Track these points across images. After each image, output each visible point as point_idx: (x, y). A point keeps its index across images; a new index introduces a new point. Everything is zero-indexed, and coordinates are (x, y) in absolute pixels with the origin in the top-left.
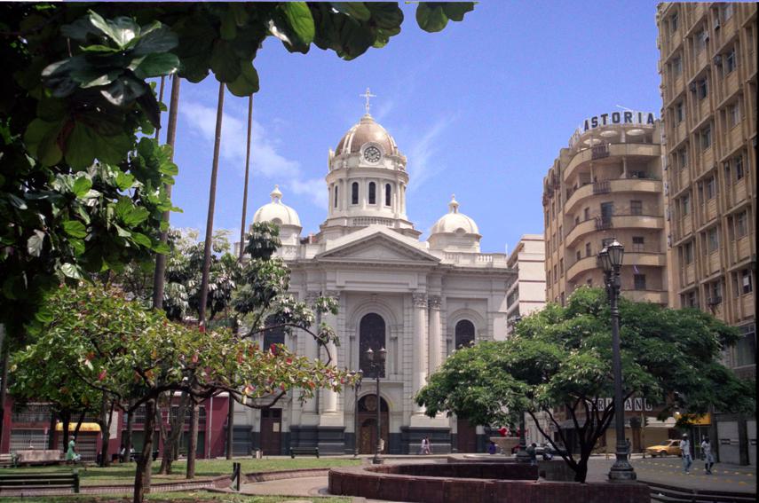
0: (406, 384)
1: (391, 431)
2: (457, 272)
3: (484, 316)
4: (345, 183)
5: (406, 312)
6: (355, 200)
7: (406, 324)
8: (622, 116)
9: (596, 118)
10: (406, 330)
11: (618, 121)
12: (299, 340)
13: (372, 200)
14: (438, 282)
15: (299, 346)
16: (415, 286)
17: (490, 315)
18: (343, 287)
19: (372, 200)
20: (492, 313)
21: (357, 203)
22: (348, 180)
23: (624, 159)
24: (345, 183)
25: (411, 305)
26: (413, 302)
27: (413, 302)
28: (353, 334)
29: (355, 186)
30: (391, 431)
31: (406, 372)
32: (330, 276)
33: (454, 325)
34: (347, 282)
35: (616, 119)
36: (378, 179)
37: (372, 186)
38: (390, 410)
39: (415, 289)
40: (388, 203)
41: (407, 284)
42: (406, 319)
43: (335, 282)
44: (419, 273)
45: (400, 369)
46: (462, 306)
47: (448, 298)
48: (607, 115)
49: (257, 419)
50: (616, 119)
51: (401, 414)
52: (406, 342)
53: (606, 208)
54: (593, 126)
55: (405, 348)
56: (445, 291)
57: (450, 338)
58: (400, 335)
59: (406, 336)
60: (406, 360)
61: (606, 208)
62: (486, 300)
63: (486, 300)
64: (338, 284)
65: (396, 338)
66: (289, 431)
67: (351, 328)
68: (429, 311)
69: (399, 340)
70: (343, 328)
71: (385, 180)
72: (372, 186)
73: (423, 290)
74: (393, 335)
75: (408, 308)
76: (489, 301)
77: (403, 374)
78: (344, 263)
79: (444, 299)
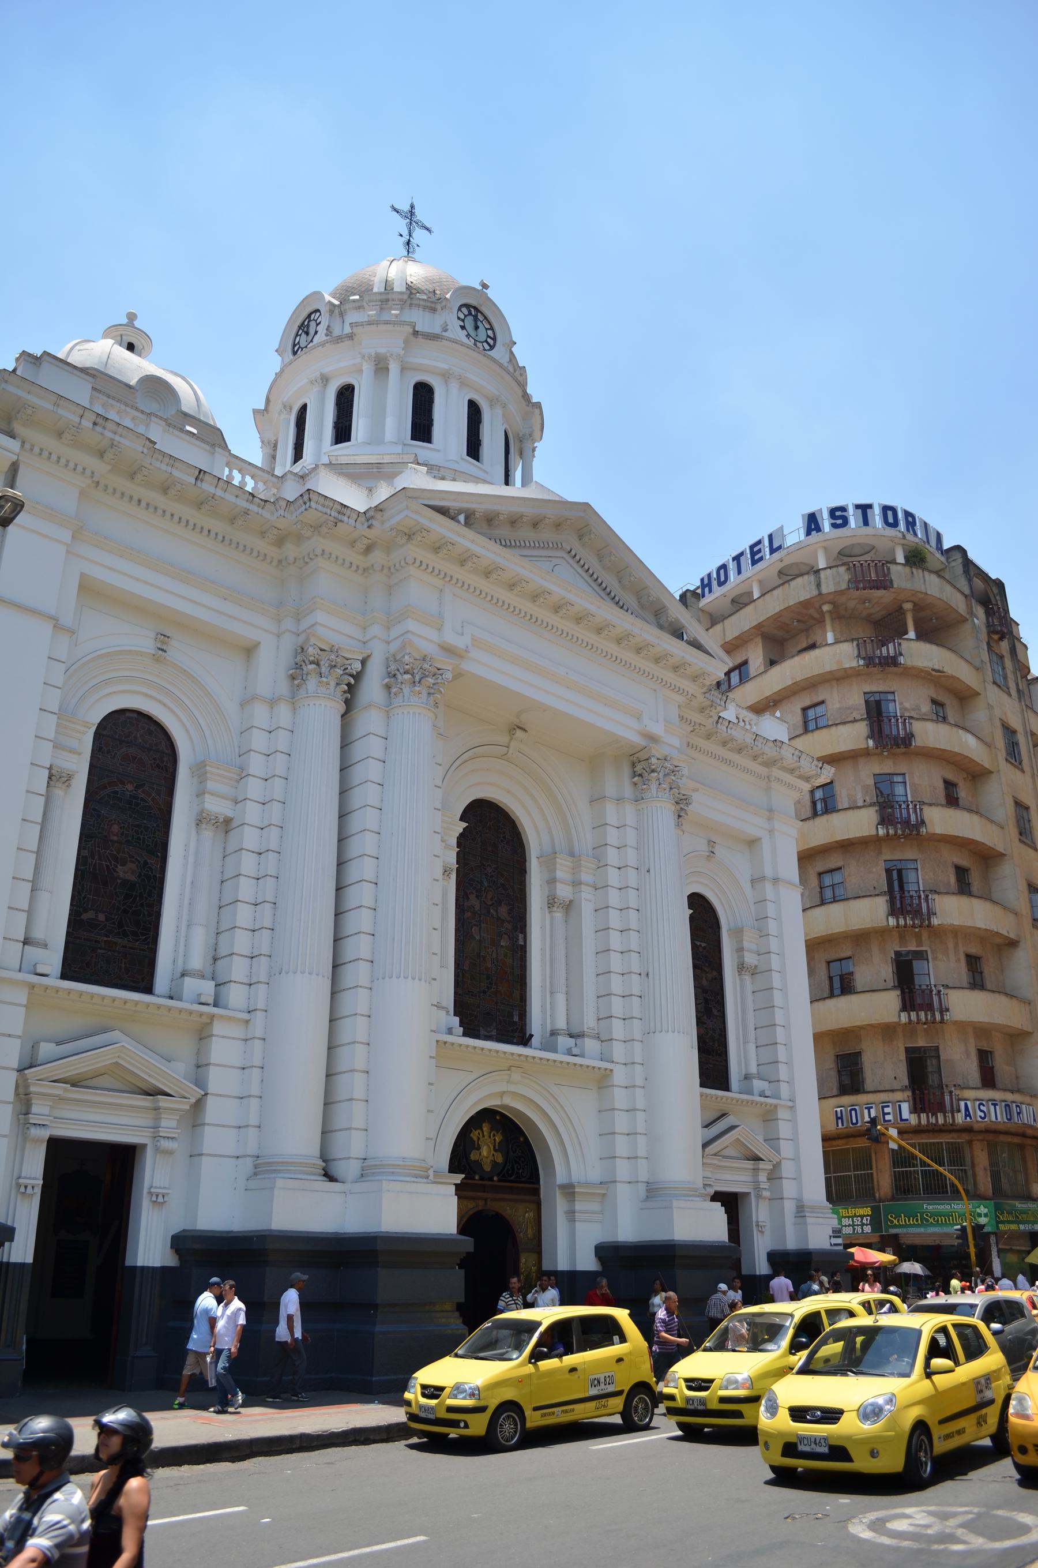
0: (619, 1076)
5: (611, 813)
8: (900, 515)
9: (843, 509)
11: (895, 524)
12: (250, 838)
15: (248, 864)
23: (908, 606)
31: (618, 1029)
35: (891, 520)
48: (870, 506)
49: (20, 1188)
50: (891, 520)
53: (878, 703)
54: (834, 526)
61: (878, 703)
64: (451, 638)
66: (170, 1260)
69: (587, 910)
72: (474, 413)
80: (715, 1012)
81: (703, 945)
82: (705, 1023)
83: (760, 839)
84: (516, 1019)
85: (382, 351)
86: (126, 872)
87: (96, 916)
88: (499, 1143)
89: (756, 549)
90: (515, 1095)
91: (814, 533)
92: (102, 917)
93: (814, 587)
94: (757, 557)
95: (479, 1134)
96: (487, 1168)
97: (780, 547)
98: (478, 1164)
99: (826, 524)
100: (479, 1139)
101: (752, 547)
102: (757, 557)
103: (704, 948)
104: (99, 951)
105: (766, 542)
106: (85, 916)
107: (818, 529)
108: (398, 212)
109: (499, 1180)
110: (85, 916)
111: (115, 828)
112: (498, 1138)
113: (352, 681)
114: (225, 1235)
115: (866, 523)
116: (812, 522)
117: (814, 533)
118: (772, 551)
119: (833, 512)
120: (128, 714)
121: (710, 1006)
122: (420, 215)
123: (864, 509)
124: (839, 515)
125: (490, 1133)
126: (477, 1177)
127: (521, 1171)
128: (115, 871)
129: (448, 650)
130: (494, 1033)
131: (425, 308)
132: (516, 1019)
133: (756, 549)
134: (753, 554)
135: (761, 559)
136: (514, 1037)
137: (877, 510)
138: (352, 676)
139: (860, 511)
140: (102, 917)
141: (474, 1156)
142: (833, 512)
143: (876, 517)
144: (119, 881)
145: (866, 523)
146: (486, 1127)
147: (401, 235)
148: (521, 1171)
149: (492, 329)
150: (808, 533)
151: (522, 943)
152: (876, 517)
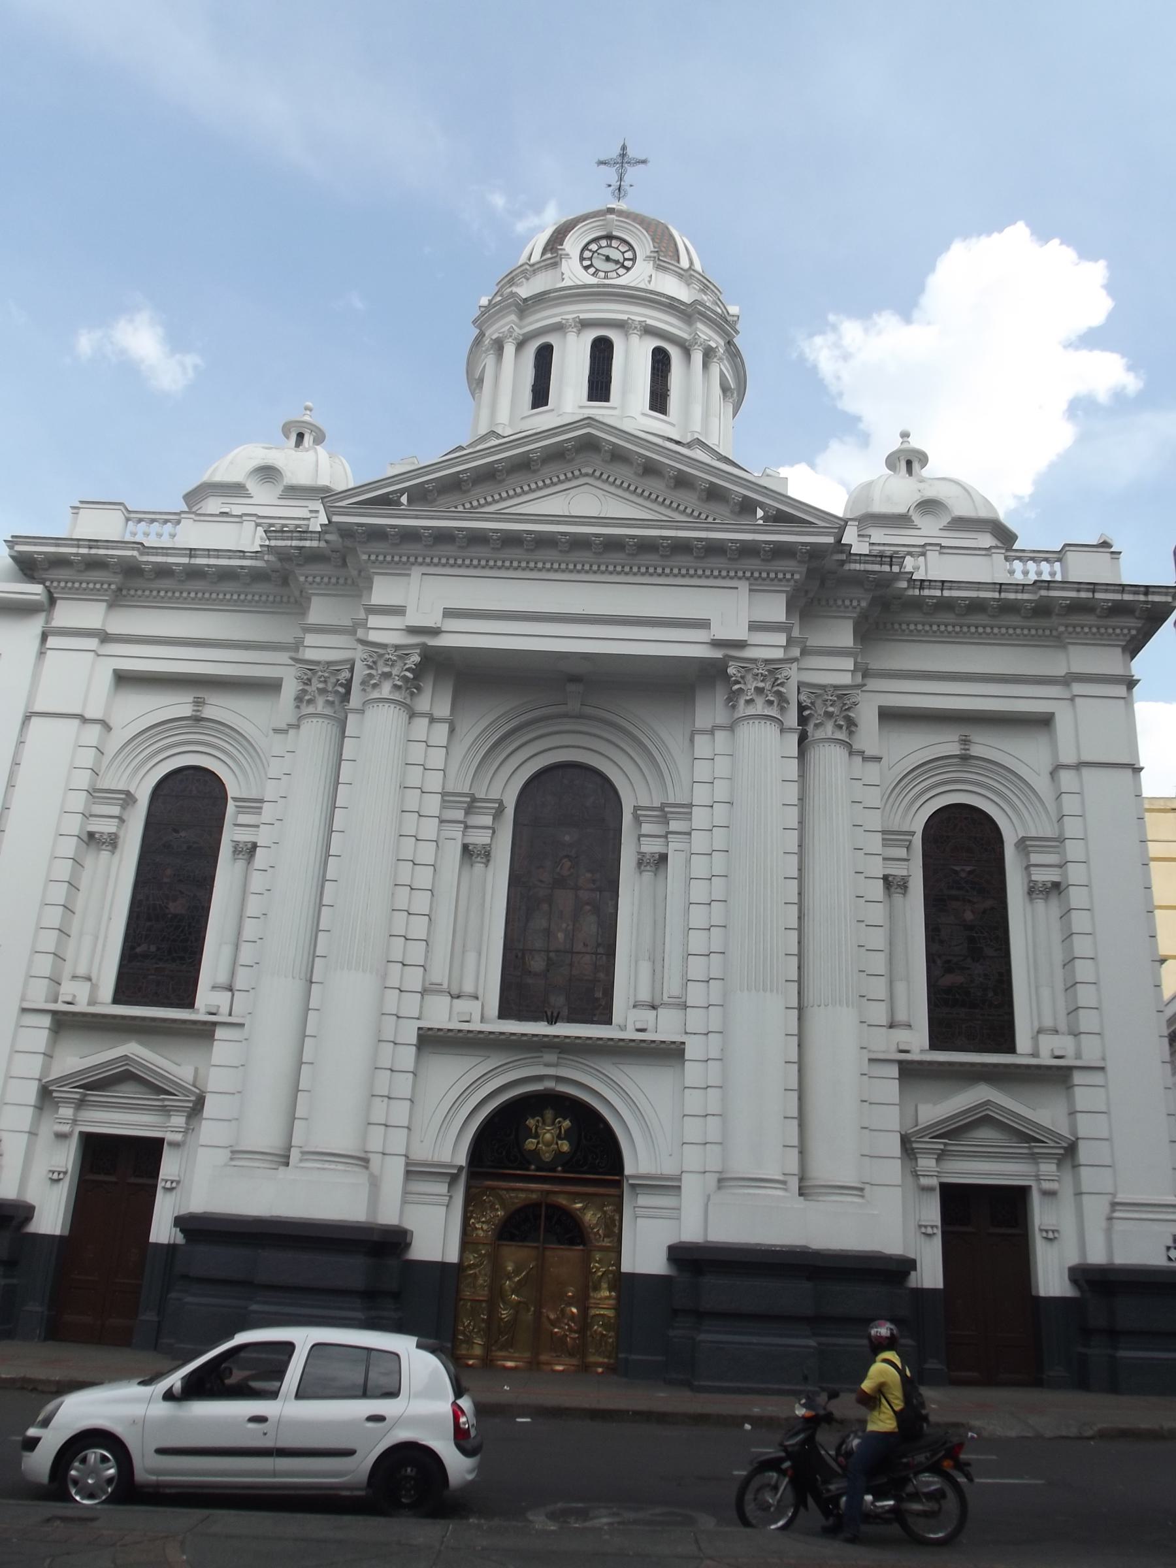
1: (626, 1267)
2: (917, 604)
3: (1041, 783)
4: (509, 349)
6: (540, 396)
7: (701, 795)
10: (700, 817)
13: (599, 387)
14: (843, 635)
16: (739, 632)
17: (1067, 779)
18: (435, 632)
19: (599, 387)
20: (1080, 766)
21: (545, 402)
22: (520, 345)
24: (509, 349)
25: (721, 716)
26: (732, 699)
27: (732, 699)
28: (480, 838)
29: (544, 357)
30: (626, 1267)
31: (696, 995)
32: (383, 591)
33: (918, 824)
34: (449, 613)
36: (621, 325)
37: (602, 352)
38: (628, 1171)
39: (741, 645)
40: (659, 400)
41: (704, 624)
42: (702, 771)
43: (399, 611)
44: (758, 584)
45: (672, 987)
46: (946, 743)
47: (889, 716)
51: (669, 1186)
52: (699, 866)
55: (699, 892)
56: (873, 684)
57: (897, 870)
58: (674, 848)
59: (699, 842)
60: (697, 942)
62: (1044, 722)
63: (1044, 722)
65: (663, 858)
67: (470, 810)
68: (803, 739)
69: (675, 862)
70: (433, 804)
71: (649, 331)
72: (602, 352)
73: (770, 647)
74: (652, 847)
75: (712, 732)
76: (1063, 723)
77: (685, 1006)
78: (443, 537)
79: (867, 715)
80: (989, 952)
81: (968, 868)
82: (968, 969)
83: (1053, 714)
84: (599, 994)
85: (494, 337)
86: (176, 907)
87: (149, 948)
88: (565, 1131)
90: (559, 1079)
92: (153, 948)
95: (538, 1121)
96: (547, 1157)
98: (536, 1153)
100: (537, 1127)
103: (970, 873)
104: (150, 977)
106: (138, 950)
108: (605, 163)
109: (564, 1171)
110: (138, 950)
111: (169, 872)
112: (567, 1124)
113: (342, 690)
114: (330, 1223)
120: (185, 773)
121: (978, 945)
122: (631, 153)
125: (554, 1122)
126: (533, 1167)
127: (597, 1161)
128: (167, 908)
129: (413, 630)
130: (565, 1012)
131: (547, 267)
132: (599, 994)
136: (595, 1015)
138: (341, 685)
140: (153, 948)
141: (531, 1144)
144: (170, 916)
146: (549, 1114)
147: (610, 186)
148: (597, 1161)
149: (631, 248)
151: (613, 911)
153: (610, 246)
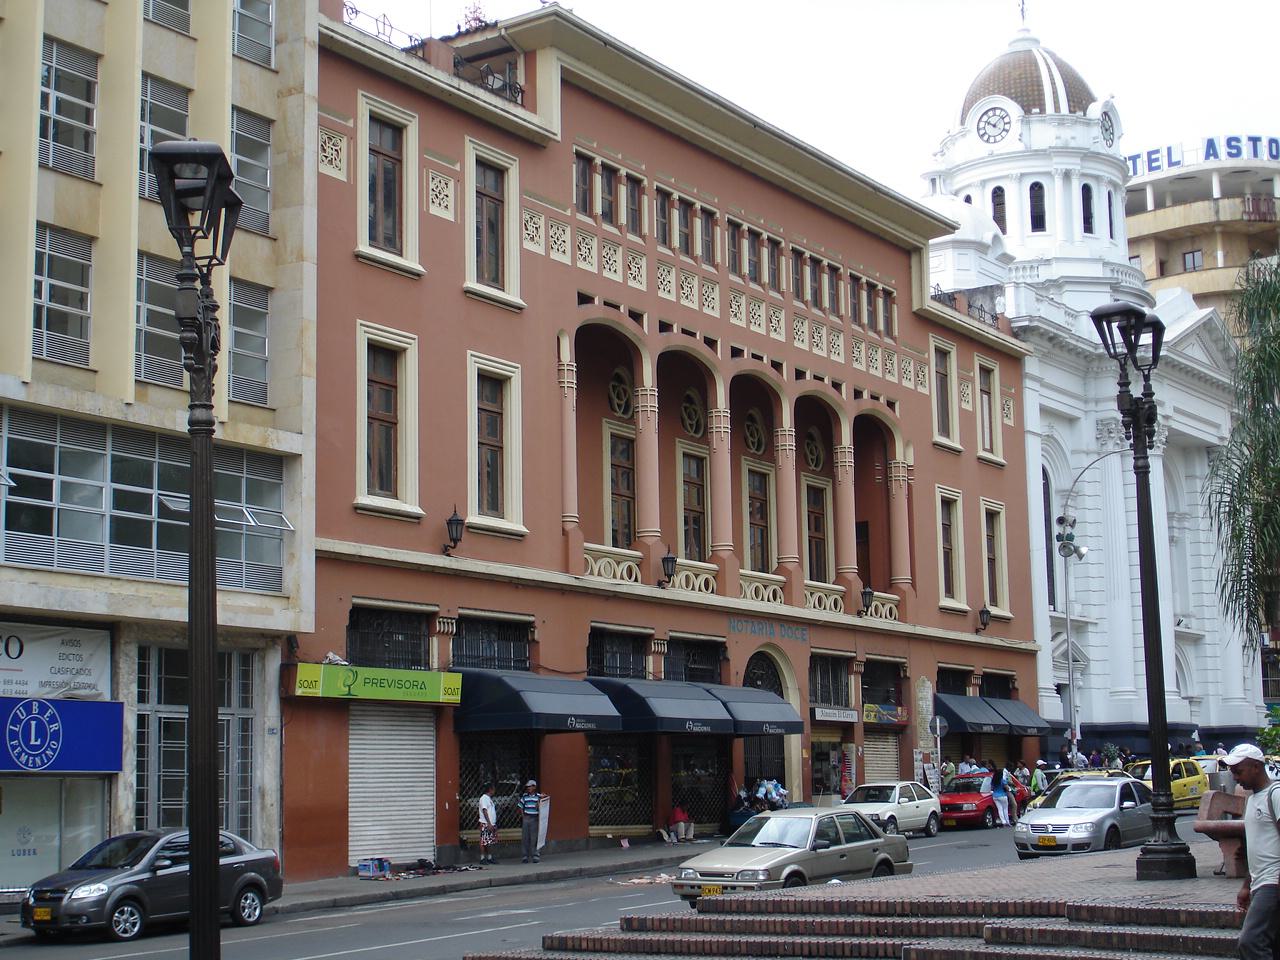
9: (1237, 140)
89: (1154, 157)
91: (1212, 158)
93: (1213, 213)
94: (1154, 165)
97: (1178, 163)
99: (1222, 149)
101: (1150, 154)
102: (1154, 165)
105: (1165, 152)
107: (1216, 155)
115: (1255, 154)
116: (1211, 148)
117: (1212, 158)
118: (1171, 164)
119: (1229, 141)
123: (1255, 140)
124: (1232, 142)
133: (1154, 157)
134: (1150, 161)
135: (1158, 168)
137: (1264, 143)
139: (1251, 143)
142: (1229, 141)
143: (1263, 147)
145: (1255, 154)
150: (1207, 157)
152: (1263, 147)
153: (994, 115)
